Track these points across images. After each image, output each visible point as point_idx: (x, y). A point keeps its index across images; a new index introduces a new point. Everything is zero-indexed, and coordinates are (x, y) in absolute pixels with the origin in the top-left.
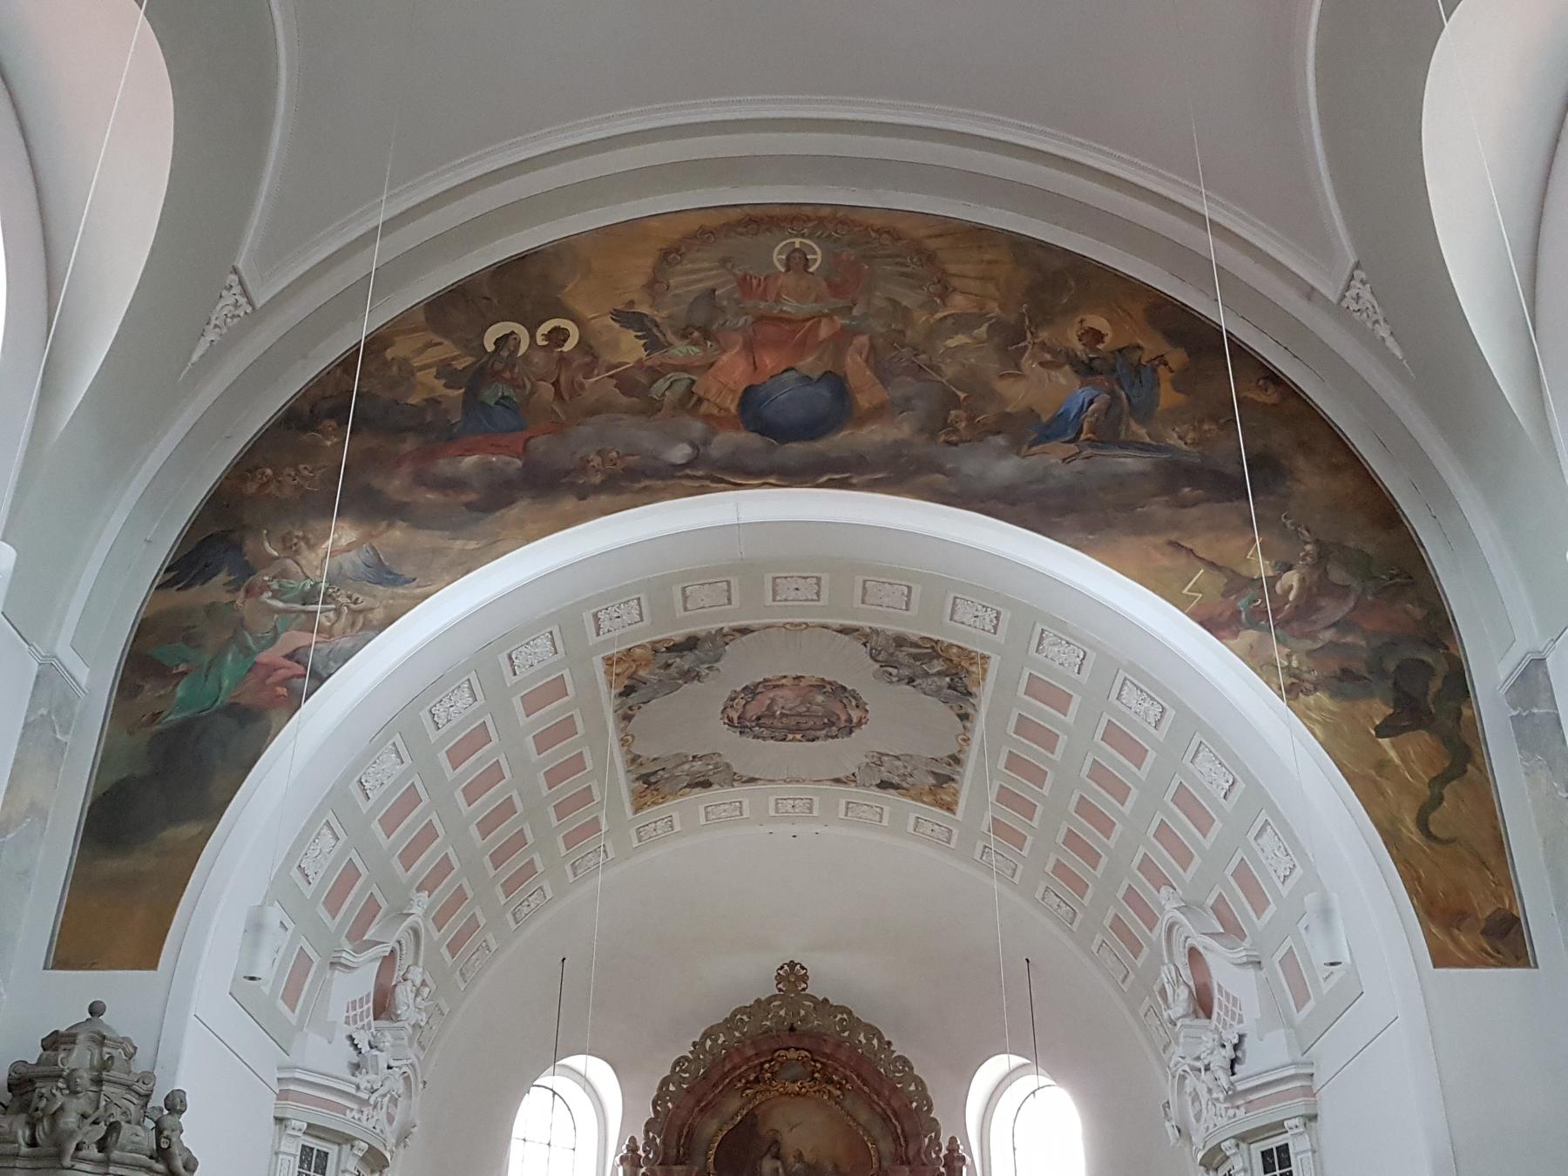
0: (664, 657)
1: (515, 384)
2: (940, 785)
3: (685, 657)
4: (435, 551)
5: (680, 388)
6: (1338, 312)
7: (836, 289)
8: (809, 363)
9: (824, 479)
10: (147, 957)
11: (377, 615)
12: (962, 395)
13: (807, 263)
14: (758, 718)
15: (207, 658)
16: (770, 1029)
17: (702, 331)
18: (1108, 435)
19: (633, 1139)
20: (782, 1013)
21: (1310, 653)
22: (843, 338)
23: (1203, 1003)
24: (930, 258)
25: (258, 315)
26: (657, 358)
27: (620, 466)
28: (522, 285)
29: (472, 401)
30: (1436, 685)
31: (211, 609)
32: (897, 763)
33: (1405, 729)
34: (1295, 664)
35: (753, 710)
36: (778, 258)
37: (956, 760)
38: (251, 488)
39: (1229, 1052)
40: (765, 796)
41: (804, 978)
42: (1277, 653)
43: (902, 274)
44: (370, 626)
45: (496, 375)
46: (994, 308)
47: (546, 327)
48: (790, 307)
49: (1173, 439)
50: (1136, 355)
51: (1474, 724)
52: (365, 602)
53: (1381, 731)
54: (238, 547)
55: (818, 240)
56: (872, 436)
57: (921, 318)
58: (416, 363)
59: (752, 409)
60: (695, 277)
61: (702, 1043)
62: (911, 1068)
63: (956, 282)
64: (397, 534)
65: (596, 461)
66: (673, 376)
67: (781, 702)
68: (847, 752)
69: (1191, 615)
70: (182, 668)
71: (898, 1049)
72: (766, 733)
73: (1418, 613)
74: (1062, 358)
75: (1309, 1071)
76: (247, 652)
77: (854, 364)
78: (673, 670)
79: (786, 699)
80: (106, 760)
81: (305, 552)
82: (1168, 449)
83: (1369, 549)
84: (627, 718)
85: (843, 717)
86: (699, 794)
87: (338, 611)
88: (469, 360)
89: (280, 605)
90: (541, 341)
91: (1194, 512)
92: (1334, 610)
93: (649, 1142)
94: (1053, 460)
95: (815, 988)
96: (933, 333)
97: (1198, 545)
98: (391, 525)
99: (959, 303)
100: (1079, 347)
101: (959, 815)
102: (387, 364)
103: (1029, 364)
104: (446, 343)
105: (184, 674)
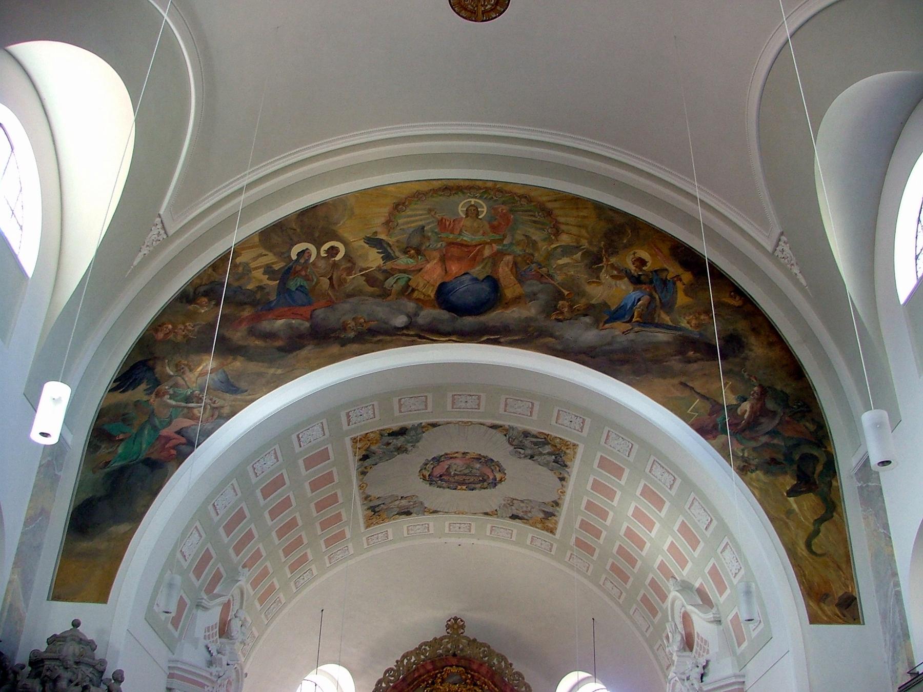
0: (386, 439)
1: (307, 278)
2: (546, 517)
3: (399, 438)
5: (402, 283)
6: (772, 255)
7: (494, 228)
8: (478, 271)
9: (485, 338)
10: (102, 596)
11: (226, 411)
12: (566, 293)
13: (478, 214)
14: (441, 476)
15: (134, 431)
16: (441, 655)
18: (648, 320)
20: (449, 646)
21: (754, 449)
22: (497, 257)
23: (688, 643)
24: (549, 213)
25: (169, 239)
26: (389, 265)
27: (366, 326)
28: (314, 223)
29: (283, 289)
30: (819, 468)
31: (137, 404)
32: (522, 505)
33: (801, 493)
34: (746, 455)
35: (438, 471)
36: (461, 210)
37: (556, 504)
38: (160, 336)
39: (700, 670)
40: (444, 522)
41: (463, 627)
42: (738, 449)
43: (535, 222)
44: (221, 416)
45: (297, 273)
46: (585, 244)
47: (326, 246)
48: (467, 238)
49: (684, 324)
50: (664, 275)
51: (838, 489)
52: (219, 402)
53: (791, 493)
54: (152, 369)
56: (513, 314)
57: (544, 247)
58: (253, 265)
59: (444, 296)
60: (415, 217)
61: (402, 661)
62: (523, 678)
63: (563, 227)
64: (238, 364)
65: (352, 324)
66: (397, 275)
67: (454, 467)
68: (492, 497)
69: (692, 425)
70: (121, 437)
71: (517, 667)
72: (445, 484)
73: (812, 427)
75: (742, 680)
76: (155, 429)
77: (504, 272)
78: (391, 447)
79: (458, 465)
80: (81, 486)
81: (188, 373)
82: (680, 329)
83: (788, 391)
84: (364, 473)
85: (491, 477)
86: (404, 519)
88: (282, 264)
89: (173, 403)
90: (323, 254)
91: (695, 366)
92: (768, 425)
95: (469, 632)
96: (550, 255)
97: (696, 385)
98: (234, 359)
99: (565, 239)
101: (558, 536)
103: (603, 275)
104: (270, 254)
105: (122, 440)
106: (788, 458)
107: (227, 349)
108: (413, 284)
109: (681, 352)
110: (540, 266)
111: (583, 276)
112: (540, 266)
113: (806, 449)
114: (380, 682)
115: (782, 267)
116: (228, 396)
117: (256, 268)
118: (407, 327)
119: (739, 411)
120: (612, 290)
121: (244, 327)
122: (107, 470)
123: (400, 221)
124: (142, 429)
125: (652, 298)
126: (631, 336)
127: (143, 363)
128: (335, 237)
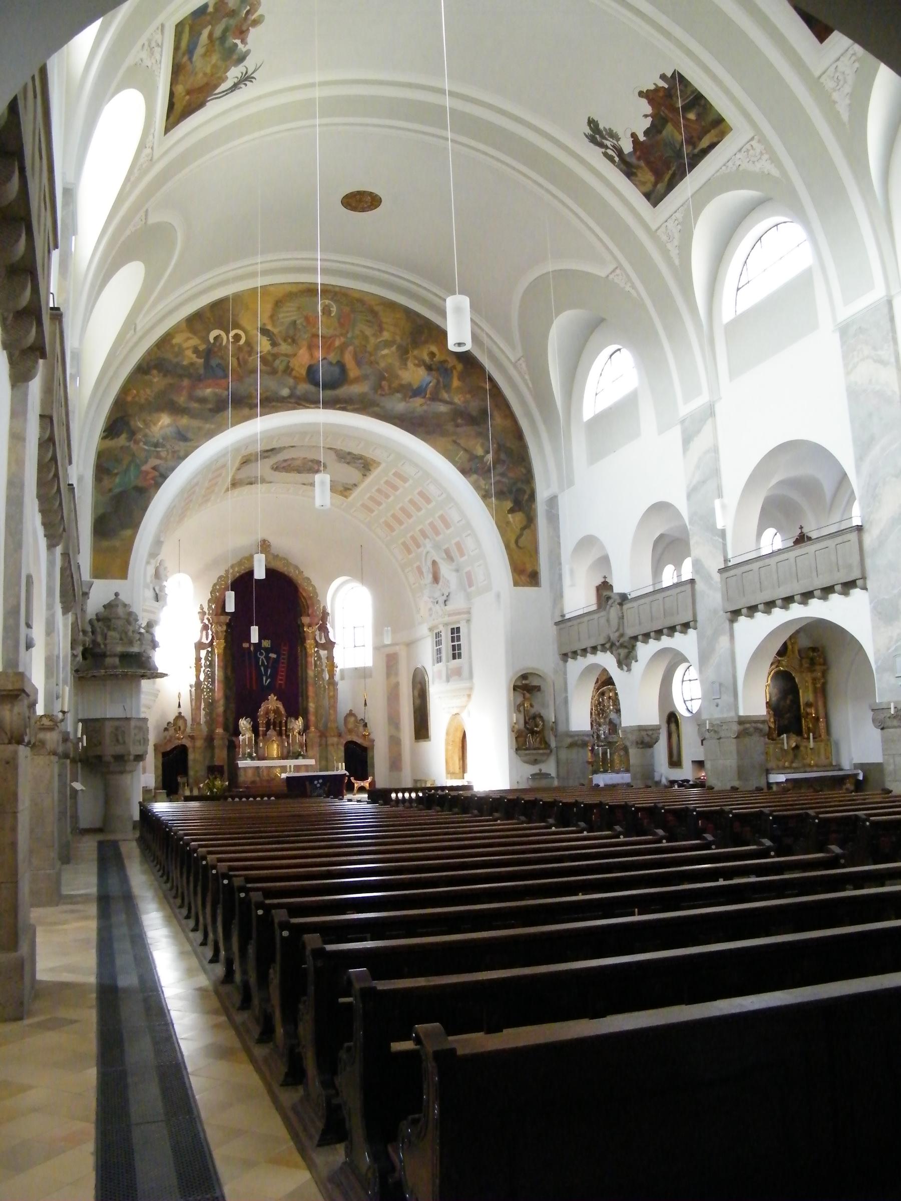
1: (222, 358)
4: (200, 429)
5: (284, 364)
6: (515, 365)
7: (341, 325)
8: (333, 357)
12: (386, 375)
13: (330, 312)
17: (293, 340)
18: (435, 398)
19: (202, 608)
23: (436, 579)
24: (374, 313)
26: (276, 350)
29: (207, 364)
31: (122, 448)
35: (285, 464)
39: (445, 598)
41: (269, 546)
42: (482, 483)
43: (367, 321)
46: (398, 338)
47: (232, 334)
49: (456, 400)
51: (535, 511)
52: (177, 448)
54: (127, 424)
55: (336, 301)
56: (356, 389)
57: (373, 340)
58: (185, 345)
59: (311, 374)
60: (289, 314)
63: (385, 326)
64: (184, 421)
66: (282, 358)
69: (458, 468)
70: (116, 471)
71: (307, 574)
73: (524, 471)
74: (421, 363)
77: (348, 359)
79: (298, 463)
80: (96, 506)
87: (167, 451)
89: (146, 447)
90: (231, 340)
91: (459, 430)
93: (210, 607)
94: (418, 405)
96: (377, 348)
97: (462, 442)
98: (182, 417)
99: (386, 335)
100: (426, 358)
102: (173, 346)
103: (410, 365)
105: (116, 474)
106: (510, 492)
107: (175, 409)
108: (291, 365)
109: (454, 420)
110: (371, 354)
111: (397, 364)
112: (371, 354)
113: (519, 485)
114: (215, 585)
115: (520, 373)
116: (181, 443)
117: (188, 348)
118: (290, 396)
119: (485, 459)
120: (414, 375)
121: (185, 393)
122: (111, 494)
123: (281, 316)
124: (128, 466)
125: (438, 382)
126: (425, 407)
127: (122, 418)
128: (236, 325)
